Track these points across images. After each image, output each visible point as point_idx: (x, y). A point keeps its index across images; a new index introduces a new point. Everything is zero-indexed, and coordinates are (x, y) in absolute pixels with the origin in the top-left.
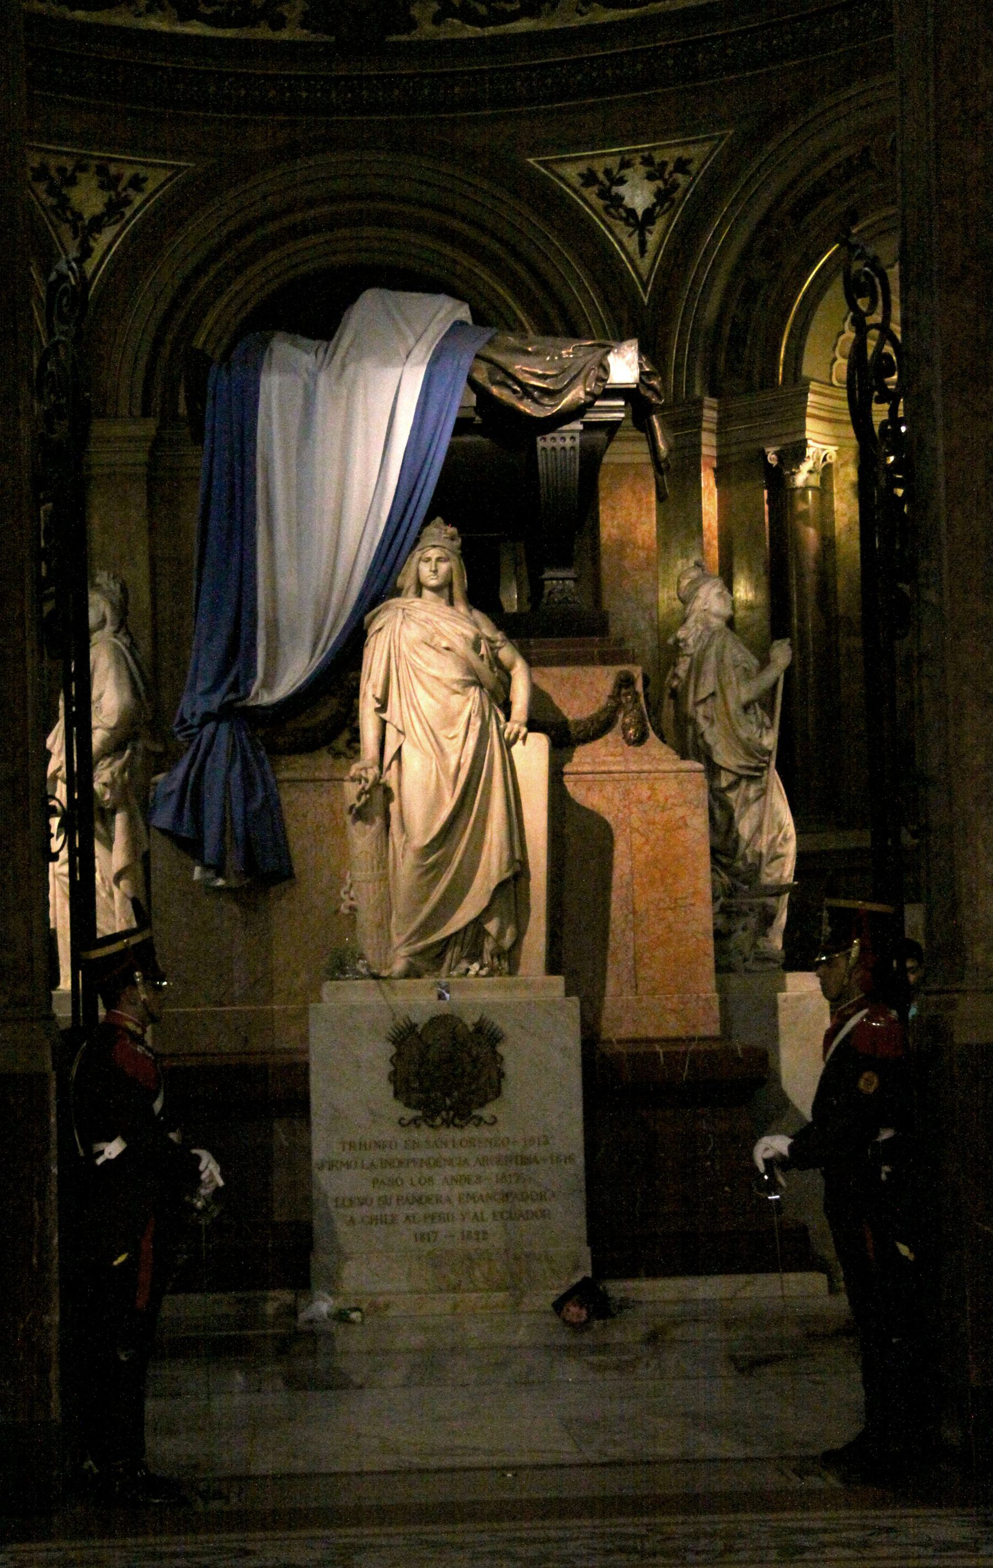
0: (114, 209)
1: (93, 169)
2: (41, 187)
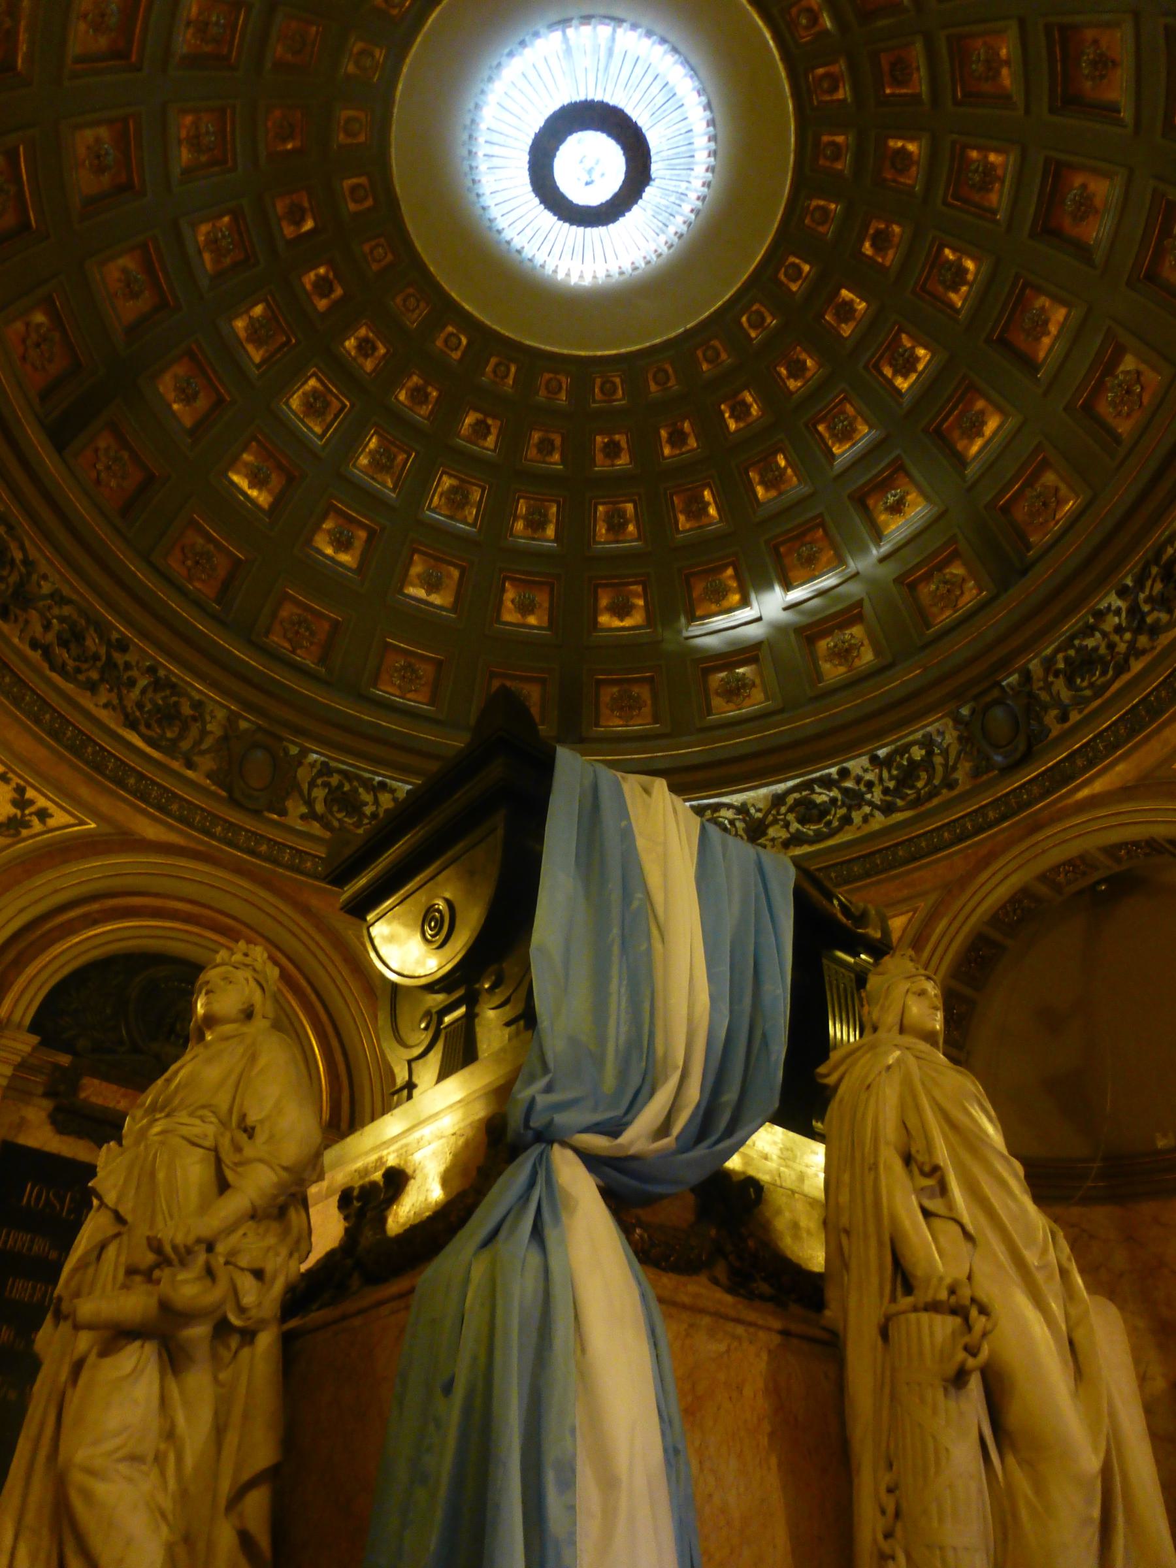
1: (14, 785)
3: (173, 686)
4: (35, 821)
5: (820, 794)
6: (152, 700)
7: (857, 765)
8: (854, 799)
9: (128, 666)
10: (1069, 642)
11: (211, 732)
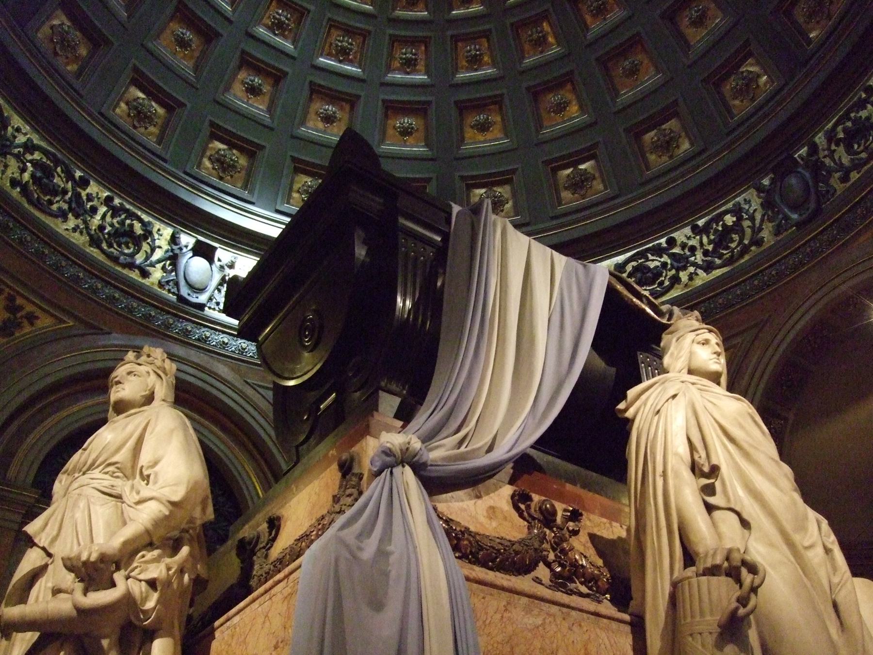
1: (6, 294)
3: (127, 211)
4: (26, 323)
5: (653, 260)
6: (112, 225)
7: (681, 235)
8: (681, 262)
9: (90, 198)
10: (846, 117)
11: (160, 247)
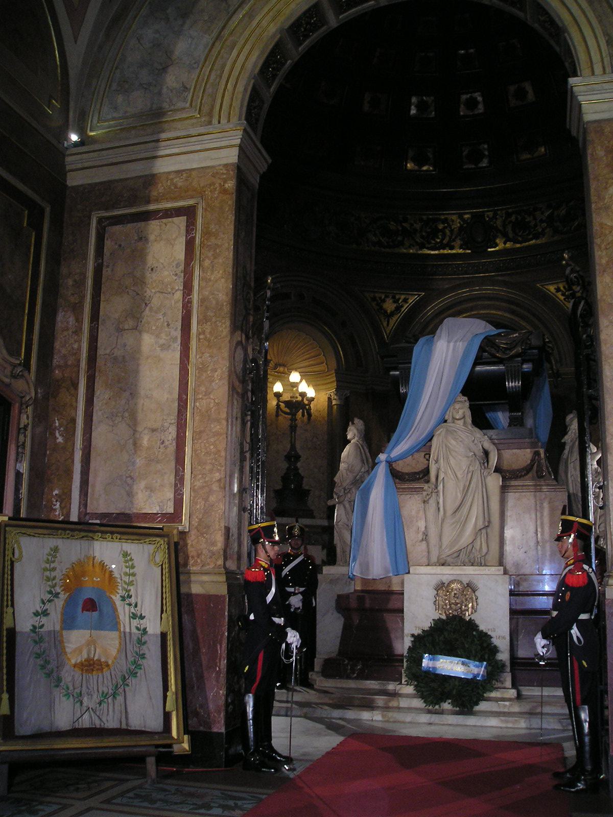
0: (398, 309)
2: (374, 304)
